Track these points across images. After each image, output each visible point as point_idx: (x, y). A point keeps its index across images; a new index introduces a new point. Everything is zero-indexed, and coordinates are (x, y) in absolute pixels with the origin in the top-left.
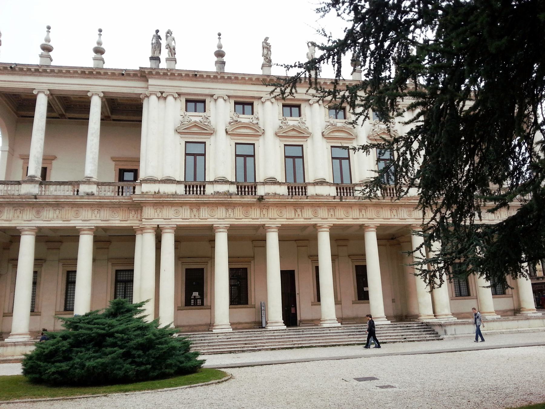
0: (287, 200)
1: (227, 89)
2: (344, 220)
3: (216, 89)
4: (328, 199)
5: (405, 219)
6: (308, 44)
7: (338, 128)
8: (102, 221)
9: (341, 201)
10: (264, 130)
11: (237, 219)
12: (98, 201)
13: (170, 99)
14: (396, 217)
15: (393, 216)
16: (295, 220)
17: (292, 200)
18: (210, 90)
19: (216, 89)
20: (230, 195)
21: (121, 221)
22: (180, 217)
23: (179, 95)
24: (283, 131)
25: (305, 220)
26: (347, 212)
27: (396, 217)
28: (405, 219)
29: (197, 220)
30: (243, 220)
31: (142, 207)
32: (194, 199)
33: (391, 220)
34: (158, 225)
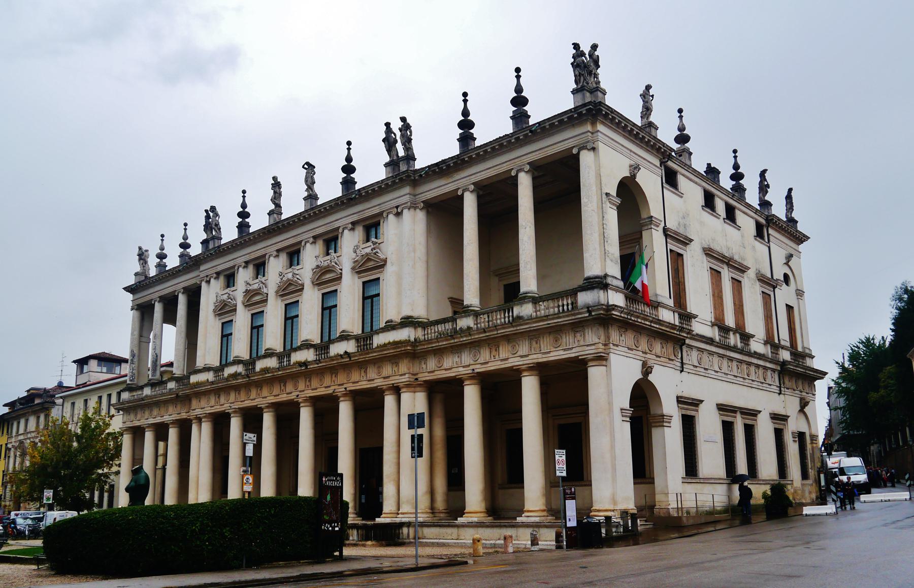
0: (267, 375)
1: (244, 255)
2: (318, 390)
3: (238, 258)
4: (296, 368)
5: (373, 380)
6: (303, 167)
7: (325, 269)
8: (178, 414)
9: (307, 368)
10: (266, 293)
11: (241, 401)
12: (169, 397)
13: (212, 280)
14: (365, 378)
15: (362, 378)
16: (280, 396)
17: (270, 375)
18: (235, 260)
19: (238, 258)
20: (235, 376)
21: (186, 413)
22: (210, 405)
23: (218, 274)
24: (281, 289)
25: (288, 396)
26: (321, 380)
27: (365, 378)
28: (373, 380)
29: (218, 407)
30: (246, 402)
31: (190, 401)
32: (209, 387)
33: (360, 383)
34: (196, 415)
